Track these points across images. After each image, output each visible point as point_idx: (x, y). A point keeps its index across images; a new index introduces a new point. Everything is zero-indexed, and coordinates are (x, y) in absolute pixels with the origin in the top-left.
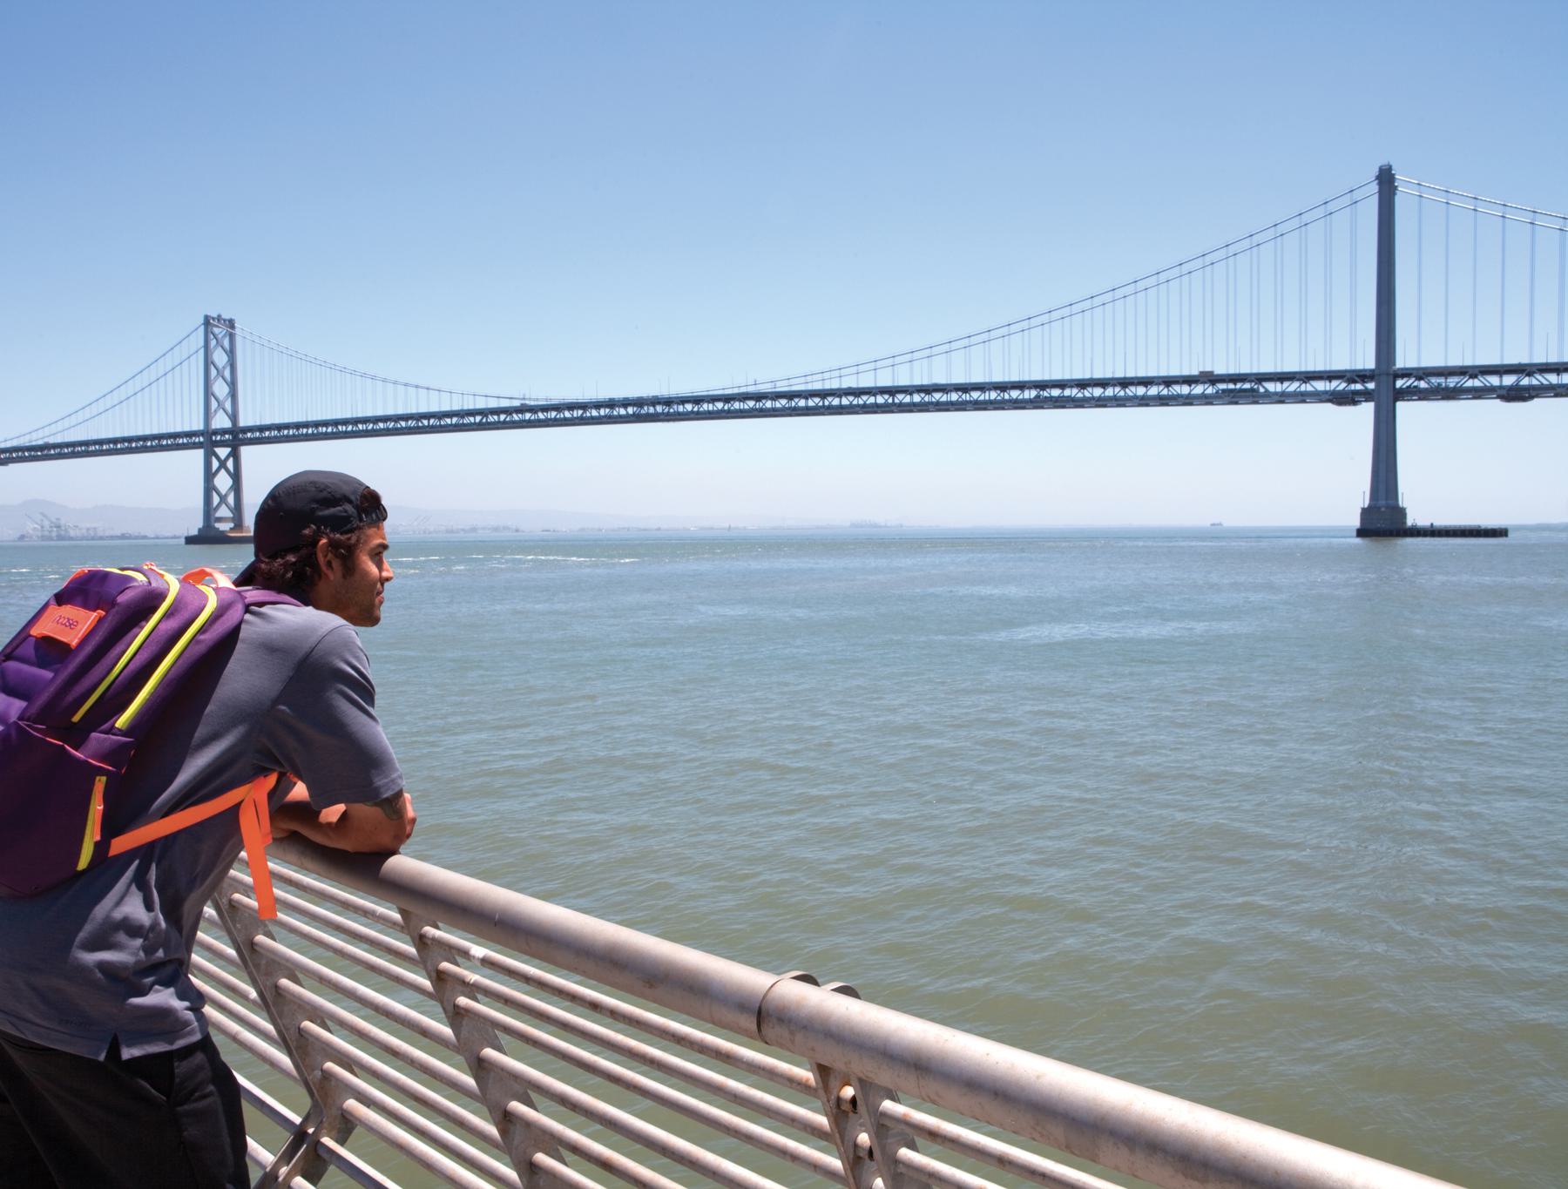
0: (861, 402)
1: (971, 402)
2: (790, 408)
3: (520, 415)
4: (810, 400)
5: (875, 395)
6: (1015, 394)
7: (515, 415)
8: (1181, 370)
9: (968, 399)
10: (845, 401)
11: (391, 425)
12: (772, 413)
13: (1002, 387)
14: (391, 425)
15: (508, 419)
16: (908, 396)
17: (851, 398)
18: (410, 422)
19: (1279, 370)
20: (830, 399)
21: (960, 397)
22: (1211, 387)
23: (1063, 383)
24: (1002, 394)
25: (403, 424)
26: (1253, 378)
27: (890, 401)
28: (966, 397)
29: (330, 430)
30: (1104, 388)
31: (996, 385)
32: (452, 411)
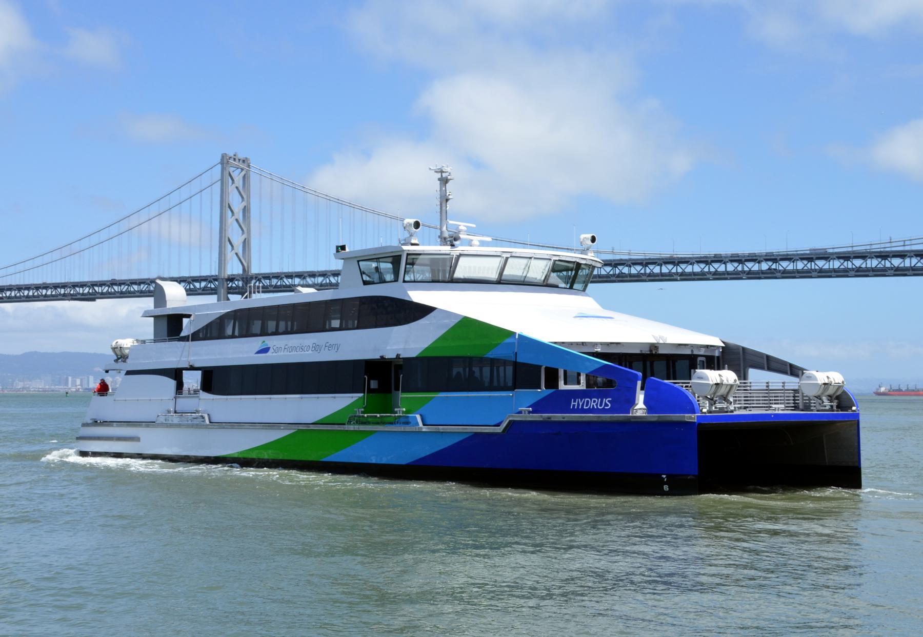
0: (712, 270)
1: (853, 269)
2: (614, 275)
3: (290, 280)
4: (632, 268)
5: (692, 264)
6: (896, 262)
7: (285, 280)
8: (211, 272)
9: (813, 268)
10: (665, 270)
11: (124, 288)
12: (661, 278)
13: (645, 263)
14: (105, 289)
15: (279, 283)
16: (757, 264)
17: (670, 267)
18: (142, 286)
19: (81, 280)
20: (651, 267)
21: (806, 265)
22: (707, 267)
23: (337, 273)
24: (883, 262)
25: (136, 287)
26: (51, 286)
27: (740, 268)
28: (849, 265)
29: (87, 290)
30: (46, 289)
31: (311, 274)
32: (200, 277)
